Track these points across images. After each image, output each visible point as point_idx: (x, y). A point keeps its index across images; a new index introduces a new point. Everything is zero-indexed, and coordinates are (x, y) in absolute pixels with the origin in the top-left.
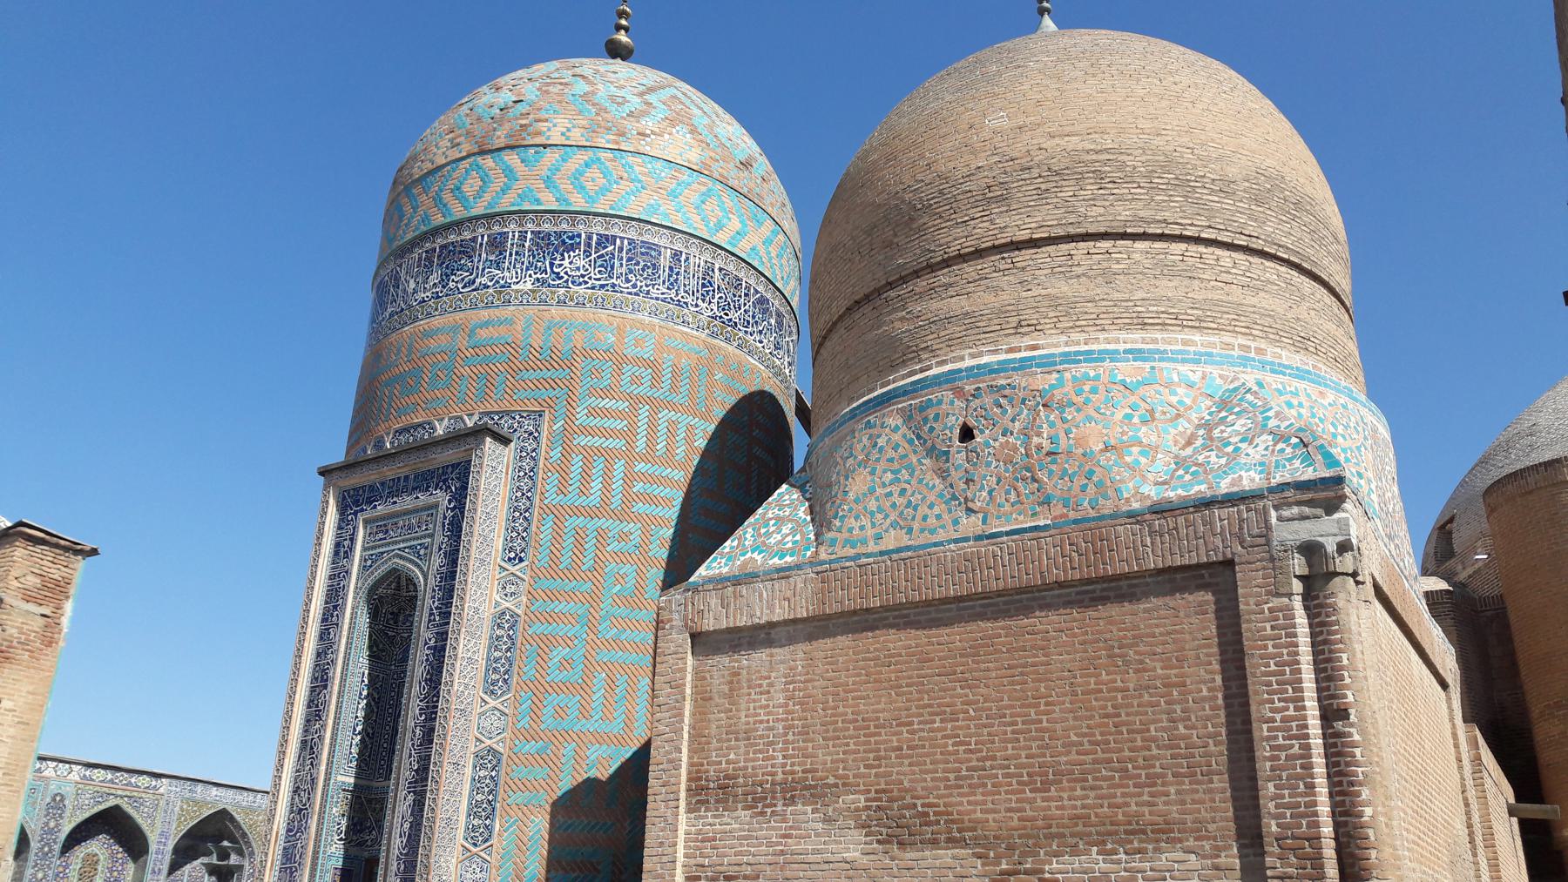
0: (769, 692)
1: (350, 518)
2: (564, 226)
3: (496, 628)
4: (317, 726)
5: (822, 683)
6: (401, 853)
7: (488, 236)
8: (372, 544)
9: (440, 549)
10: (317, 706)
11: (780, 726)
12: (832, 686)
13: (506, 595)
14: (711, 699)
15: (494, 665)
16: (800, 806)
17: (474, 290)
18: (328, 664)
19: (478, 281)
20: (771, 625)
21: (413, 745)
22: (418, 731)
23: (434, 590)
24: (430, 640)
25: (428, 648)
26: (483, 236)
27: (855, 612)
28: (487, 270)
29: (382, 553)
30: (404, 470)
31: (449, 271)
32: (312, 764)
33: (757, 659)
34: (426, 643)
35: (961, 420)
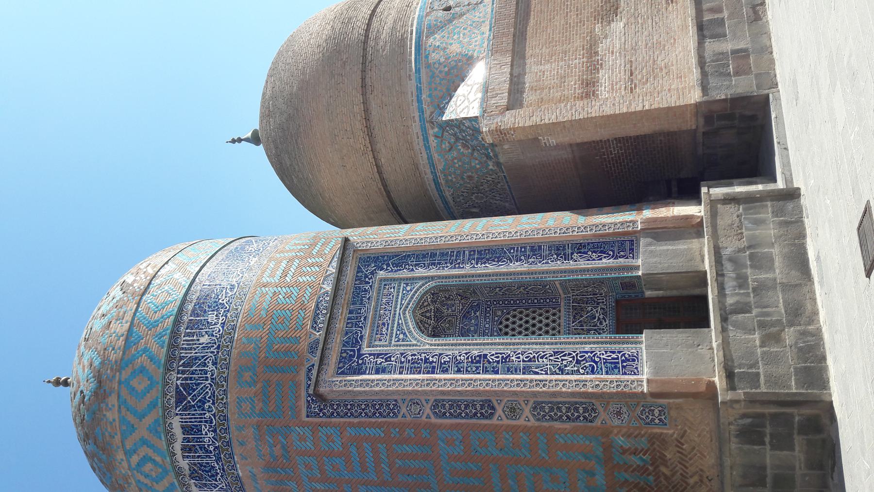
5: (544, 50)
6: (612, 257)
8: (388, 338)
9: (412, 270)
10: (498, 362)
11: (561, 64)
12: (546, 45)
16: (599, 49)
18: (468, 358)
20: (511, 74)
22: (532, 260)
26: (204, 285)
27: (514, 41)
29: (398, 324)
30: (345, 310)
32: (542, 358)
33: (529, 79)
34: (474, 267)
35: (441, 11)
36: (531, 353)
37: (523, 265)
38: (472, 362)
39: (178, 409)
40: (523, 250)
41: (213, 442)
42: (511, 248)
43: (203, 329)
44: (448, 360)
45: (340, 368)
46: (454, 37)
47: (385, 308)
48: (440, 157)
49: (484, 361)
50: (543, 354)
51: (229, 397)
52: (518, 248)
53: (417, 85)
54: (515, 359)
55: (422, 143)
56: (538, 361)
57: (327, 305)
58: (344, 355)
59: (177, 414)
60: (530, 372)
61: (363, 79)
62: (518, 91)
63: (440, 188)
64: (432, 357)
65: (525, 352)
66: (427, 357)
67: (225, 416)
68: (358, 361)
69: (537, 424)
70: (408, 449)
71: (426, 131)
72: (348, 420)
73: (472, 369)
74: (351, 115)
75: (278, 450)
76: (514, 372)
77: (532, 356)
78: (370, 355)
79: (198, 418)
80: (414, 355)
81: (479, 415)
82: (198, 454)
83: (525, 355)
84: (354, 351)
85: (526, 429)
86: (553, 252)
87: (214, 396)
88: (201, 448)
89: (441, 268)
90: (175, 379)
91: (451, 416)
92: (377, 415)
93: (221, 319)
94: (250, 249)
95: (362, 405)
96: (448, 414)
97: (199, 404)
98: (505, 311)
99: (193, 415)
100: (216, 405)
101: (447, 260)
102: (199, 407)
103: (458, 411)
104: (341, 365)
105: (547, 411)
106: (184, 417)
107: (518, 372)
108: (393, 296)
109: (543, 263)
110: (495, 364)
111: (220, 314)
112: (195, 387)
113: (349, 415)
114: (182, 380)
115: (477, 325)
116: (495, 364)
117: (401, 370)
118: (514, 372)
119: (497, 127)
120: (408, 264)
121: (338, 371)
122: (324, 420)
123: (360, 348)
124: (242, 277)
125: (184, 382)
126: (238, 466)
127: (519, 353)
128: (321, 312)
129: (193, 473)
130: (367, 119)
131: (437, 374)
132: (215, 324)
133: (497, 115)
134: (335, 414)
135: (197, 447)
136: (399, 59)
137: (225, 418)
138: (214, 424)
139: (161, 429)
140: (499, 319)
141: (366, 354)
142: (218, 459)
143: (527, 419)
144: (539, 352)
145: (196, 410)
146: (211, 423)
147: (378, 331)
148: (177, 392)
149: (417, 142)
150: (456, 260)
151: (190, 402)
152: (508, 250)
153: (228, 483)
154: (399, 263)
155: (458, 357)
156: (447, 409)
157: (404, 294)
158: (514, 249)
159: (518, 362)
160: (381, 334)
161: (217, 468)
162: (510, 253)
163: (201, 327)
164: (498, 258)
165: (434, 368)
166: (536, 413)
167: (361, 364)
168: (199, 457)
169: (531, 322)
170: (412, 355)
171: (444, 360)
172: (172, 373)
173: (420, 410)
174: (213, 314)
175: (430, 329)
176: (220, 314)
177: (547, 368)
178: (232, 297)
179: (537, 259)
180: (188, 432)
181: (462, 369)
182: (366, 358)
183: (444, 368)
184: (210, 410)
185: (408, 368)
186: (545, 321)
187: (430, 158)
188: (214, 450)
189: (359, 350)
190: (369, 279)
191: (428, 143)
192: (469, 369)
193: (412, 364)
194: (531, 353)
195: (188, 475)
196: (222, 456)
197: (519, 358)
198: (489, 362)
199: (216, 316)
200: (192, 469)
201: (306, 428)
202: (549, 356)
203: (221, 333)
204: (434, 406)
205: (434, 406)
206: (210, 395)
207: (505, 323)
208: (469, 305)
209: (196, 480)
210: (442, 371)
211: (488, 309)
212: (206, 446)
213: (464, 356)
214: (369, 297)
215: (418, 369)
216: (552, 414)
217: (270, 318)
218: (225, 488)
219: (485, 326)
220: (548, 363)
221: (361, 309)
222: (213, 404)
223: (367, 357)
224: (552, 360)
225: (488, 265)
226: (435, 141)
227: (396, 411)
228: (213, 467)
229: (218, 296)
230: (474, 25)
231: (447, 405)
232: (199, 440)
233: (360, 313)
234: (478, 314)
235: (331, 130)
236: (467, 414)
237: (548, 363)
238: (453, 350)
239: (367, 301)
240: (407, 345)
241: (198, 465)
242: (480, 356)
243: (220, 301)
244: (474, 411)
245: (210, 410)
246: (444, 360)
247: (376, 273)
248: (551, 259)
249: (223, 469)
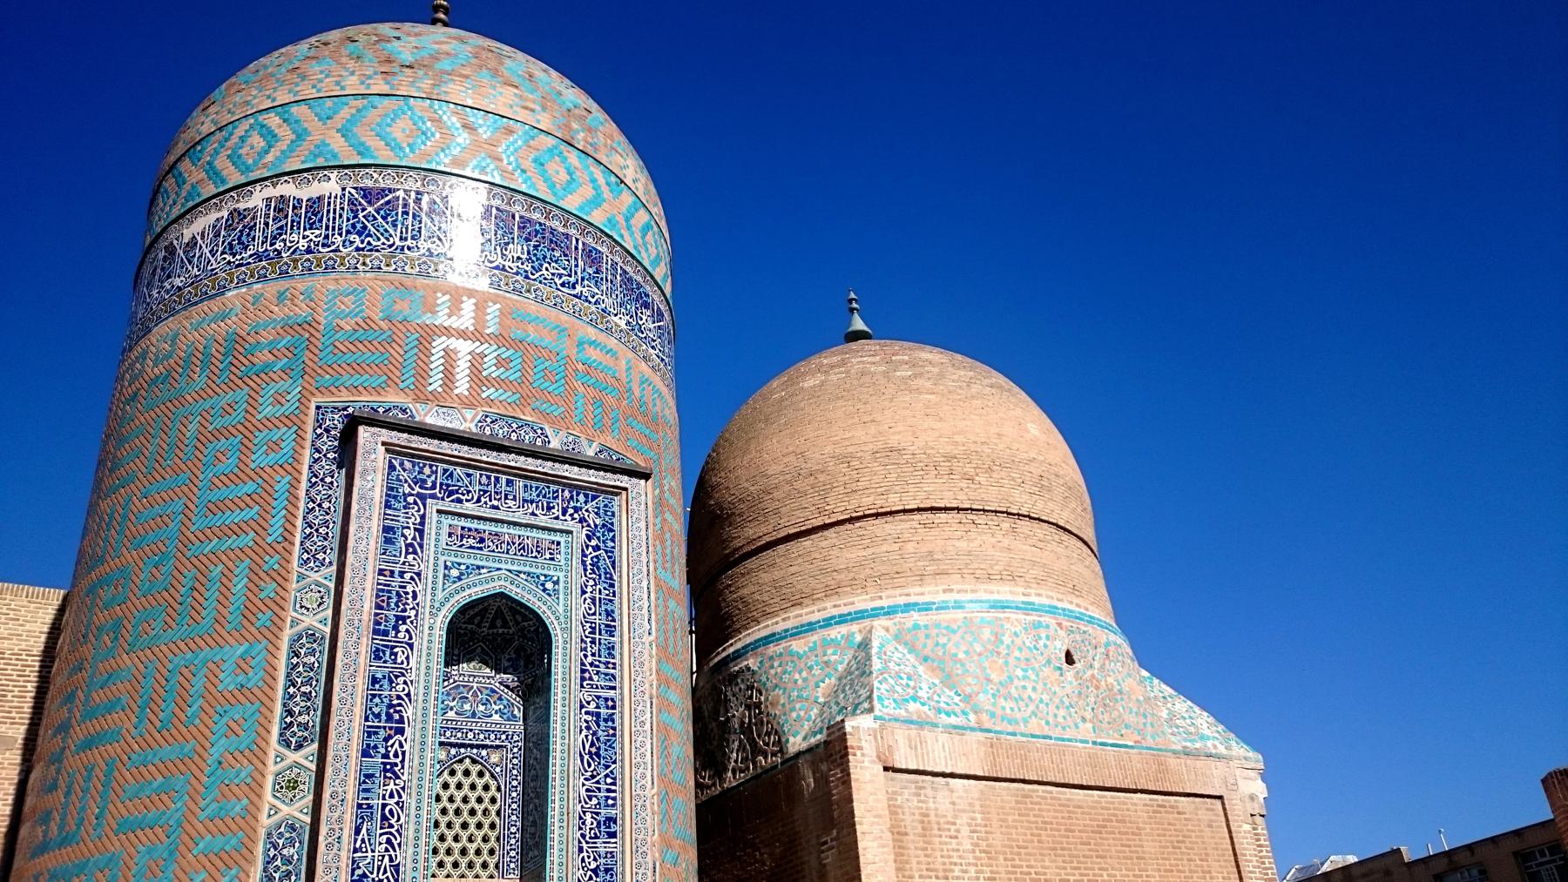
0: (956, 837)
1: (410, 499)
2: (639, 279)
4: (392, 786)
7: (584, 244)
9: (584, 592)
10: (386, 756)
11: (972, 869)
14: (906, 834)
17: (574, 296)
18: (399, 697)
19: (579, 288)
21: (583, 836)
22: (588, 817)
23: (582, 640)
24: (588, 703)
25: (587, 713)
26: (577, 240)
28: (586, 282)
29: (479, 568)
31: (540, 255)
32: (389, 842)
34: (582, 707)
36: (399, 820)
37: (580, 802)
38: (390, 706)
39: (353, 191)
40: (610, 802)
41: (290, 248)
42: (615, 779)
43: (495, 235)
44: (399, 661)
45: (402, 464)
46: (1019, 670)
47: (514, 544)
48: (811, 645)
49: (391, 728)
50: (395, 843)
51: (368, 275)
52: (614, 791)
53: (934, 603)
54: (389, 788)
55: (835, 612)
56: (381, 835)
57: (527, 441)
58: (427, 471)
59: (344, 189)
60: (362, 817)
61: (946, 509)
62: (921, 788)
63: (760, 646)
64: (407, 631)
65: (402, 808)
66: (408, 621)
67: (334, 268)
68: (412, 495)
69: (262, 833)
70: (239, 585)
71: (858, 619)
72: (304, 478)
73: (377, 705)
74: (883, 489)
75: (264, 356)
76: (364, 786)
77: (393, 821)
78: (423, 517)
79: (334, 223)
80: (415, 596)
81: (288, 720)
82: (271, 223)
83: (395, 809)
84: (434, 487)
85: (251, 813)
86: (603, 861)
87: (371, 250)
88: (281, 228)
89: (583, 645)
90: (407, 188)
91: (291, 666)
92: (308, 531)
93: (512, 265)
94: (644, 318)
95: (330, 502)
96: (295, 660)
97: (359, 226)
98: (498, 769)
99: (341, 216)
100: (355, 253)
101: (600, 656)
102: (354, 226)
103: (299, 680)
104: (408, 465)
105: (285, 852)
106: (338, 200)
107: (362, 795)
108: (536, 557)
109: (580, 842)
110: (383, 751)
111: (522, 264)
112: (389, 219)
113: (314, 480)
114: (404, 199)
115: (474, 714)
116: (383, 751)
117: (387, 573)
118: (364, 786)
120: (596, 585)
121: (395, 459)
122: (309, 436)
123: (438, 499)
124: (590, 302)
125: (401, 202)
126: (244, 290)
127: (400, 797)
128: (514, 431)
129: (239, 214)
130: (877, 515)
131: (373, 639)
132: (502, 254)
133: (877, 748)
134: (317, 456)
135: (283, 222)
136: (978, 572)
137: (330, 269)
138: (321, 249)
139: (320, 162)
140: (482, 758)
141: (425, 509)
142: (258, 257)
143: (273, 812)
144: (400, 835)
145: (348, 220)
146: (324, 245)
147: (470, 530)
148: (383, 190)
149: (838, 603)
150: (598, 673)
151: (363, 210)
152: (611, 772)
153: (217, 273)
154: (598, 568)
155: (402, 679)
156: (305, 660)
157: (538, 577)
158: (614, 784)
159: (384, 796)
160: (462, 537)
161: (243, 255)
162: (607, 776)
163: (500, 232)
164: (598, 755)
165: (386, 633)
166: (282, 830)
167: (405, 500)
168: (267, 224)
169: (472, 821)
170: (414, 592)
171: (400, 653)
172: (419, 183)
173: (308, 609)
174: (522, 253)
175: (470, 627)
176: (522, 264)
177: (367, 852)
178: (553, 285)
179: (591, 829)
180: (311, 207)
181: (377, 686)
182: (416, 508)
183: (384, 652)
184: (347, 243)
185: (389, 585)
186: (472, 848)
187: (810, 627)
188: (276, 250)
189: (433, 496)
190: (571, 515)
191: (836, 623)
192: (377, 700)
193: (397, 592)
194: (399, 820)
195: (237, 206)
196: (264, 263)
197: (391, 796)
198: (386, 740)
199: (519, 258)
200: (246, 213)
201: (297, 404)
202: (390, 856)
203: (486, 263)
204: (314, 635)
205: (314, 635)
206: (374, 243)
207: (475, 769)
208: (515, 700)
209: (227, 221)
210: (378, 650)
211: (504, 737)
212: (284, 236)
213: (404, 690)
215: (385, 605)
216: (278, 863)
217: (507, 345)
218: (209, 268)
219: (471, 730)
220: (376, 854)
221: (514, 499)
222: (358, 249)
223: (419, 510)
224: (382, 861)
225: (585, 732)
226: (839, 637)
227: (312, 564)
228: (246, 248)
229: (556, 262)
230: (1041, 705)
231: (313, 659)
232: (296, 225)
233: (506, 498)
234: (496, 717)
235: (858, 455)
236: (292, 697)
237: (376, 854)
238: (418, 669)
239: (530, 511)
240: (434, 583)
241: (252, 224)
242: (401, 721)
243: (546, 265)
244: (297, 710)
245: (347, 243)
246: (400, 653)
247: (583, 527)
248: (589, 857)
249: (238, 266)
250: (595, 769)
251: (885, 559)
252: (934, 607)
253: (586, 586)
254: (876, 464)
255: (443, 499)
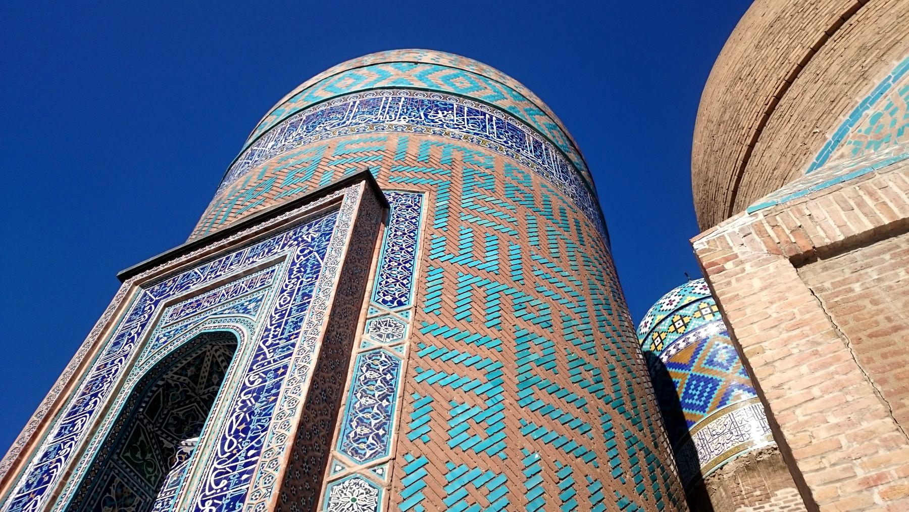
3: (364, 369)
13: (380, 336)
15: (361, 415)
24: (252, 383)
26: (354, 103)
119: (713, 264)
214: (256, 262)
225: (235, 414)
250: (237, 447)
251: (813, 106)
252: (890, 81)
253: (287, 286)
254: (763, 52)
255: (174, 294)
